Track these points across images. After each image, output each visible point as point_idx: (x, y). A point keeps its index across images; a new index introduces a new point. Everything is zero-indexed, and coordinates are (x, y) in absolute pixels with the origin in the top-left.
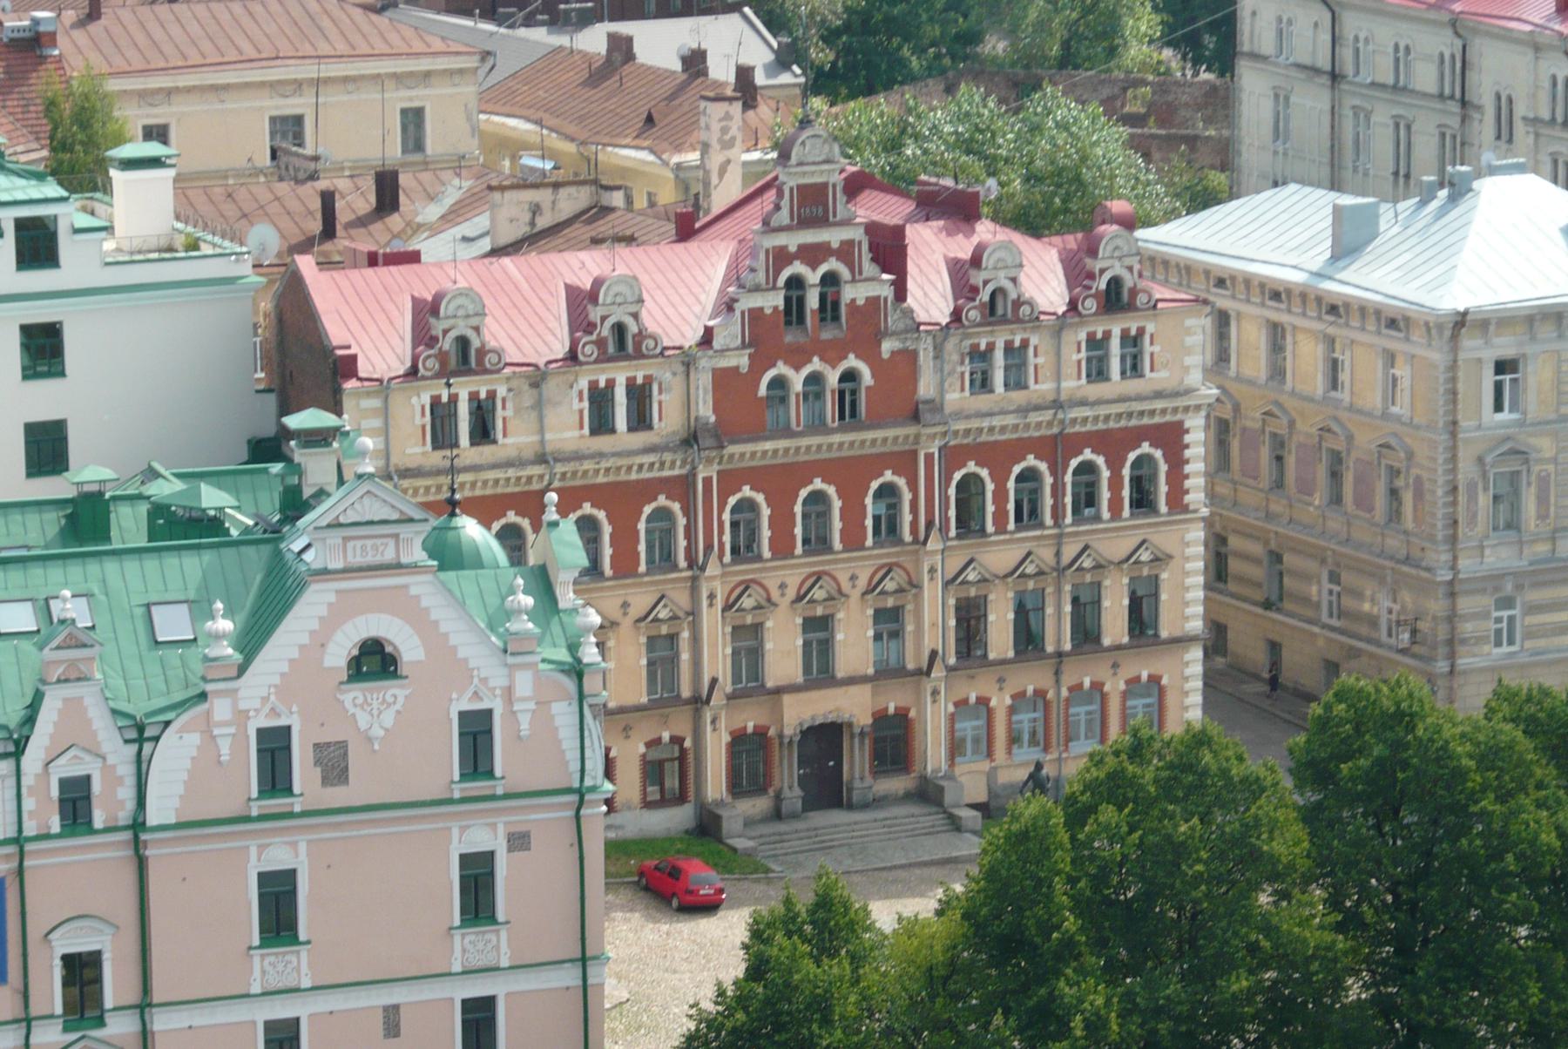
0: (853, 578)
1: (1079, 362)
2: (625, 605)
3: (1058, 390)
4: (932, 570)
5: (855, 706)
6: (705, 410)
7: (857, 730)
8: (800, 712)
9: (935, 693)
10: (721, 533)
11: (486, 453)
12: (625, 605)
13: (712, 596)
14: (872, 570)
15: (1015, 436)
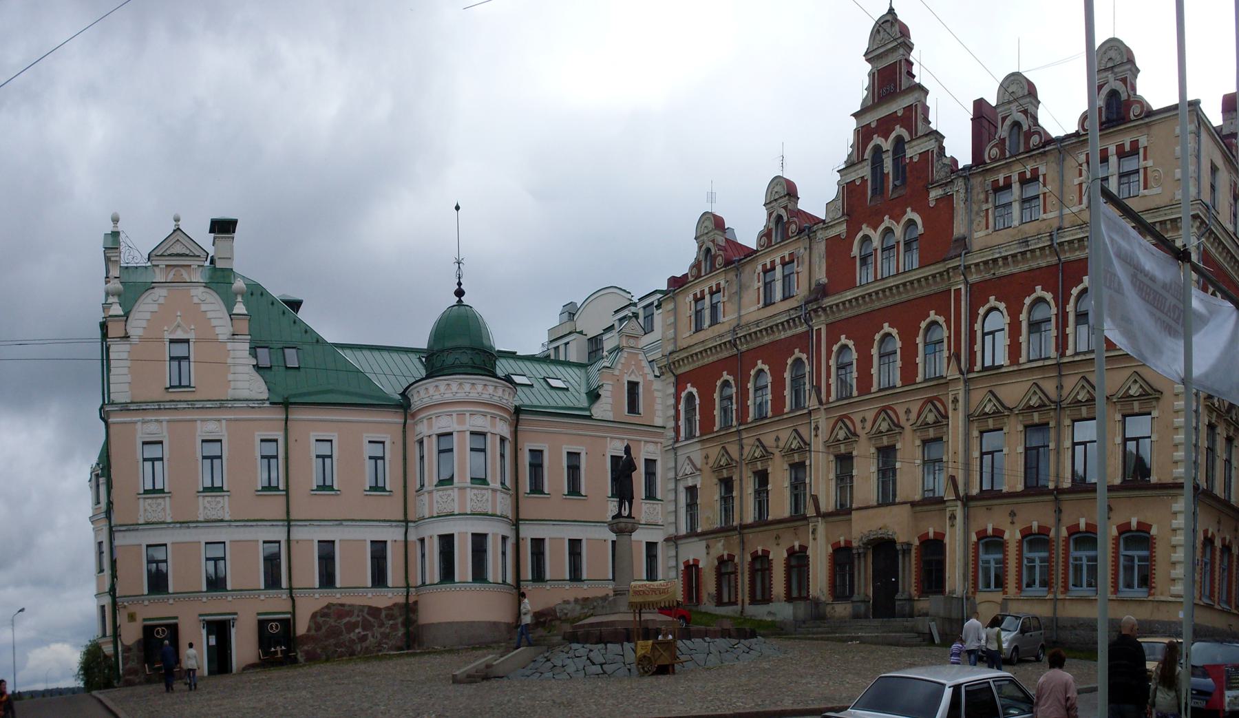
0: (908, 411)
1: (1080, 184)
2: (777, 439)
3: (1061, 216)
4: (955, 401)
5: (898, 524)
6: (821, 276)
7: (899, 547)
8: (862, 527)
9: (953, 517)
10: (828, 376)
11: (718, 329)
12: (777, 439)
13: (817, 428)
14: (920, 403)
15: (1025, 267)
